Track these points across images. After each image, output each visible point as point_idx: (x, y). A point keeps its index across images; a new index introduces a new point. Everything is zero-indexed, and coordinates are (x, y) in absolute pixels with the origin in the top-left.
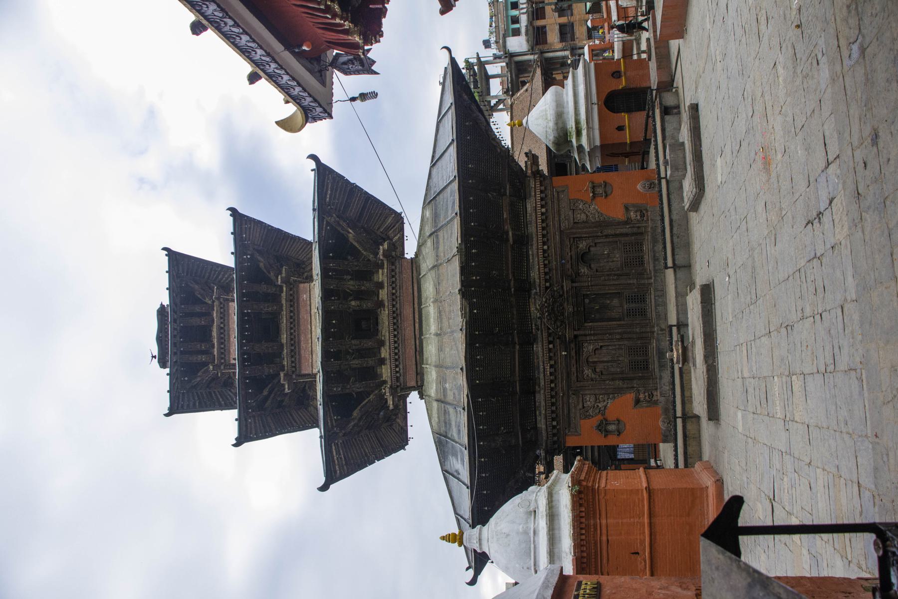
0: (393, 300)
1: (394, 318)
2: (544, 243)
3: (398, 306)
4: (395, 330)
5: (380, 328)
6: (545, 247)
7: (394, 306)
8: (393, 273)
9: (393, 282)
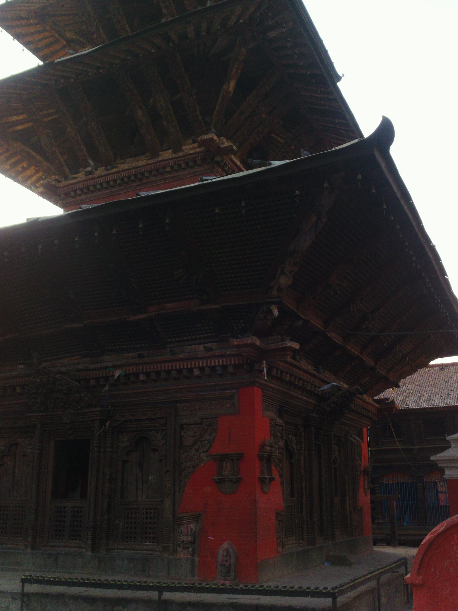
0: (157, 170)
1: (136, 175)
2: (147, 374)
3: (152, 179)
4: (122, 179)
5: (128, 160)
6: (142, 377)
7: (150, 172)
8: (191, 164)
9: (180, 165)
